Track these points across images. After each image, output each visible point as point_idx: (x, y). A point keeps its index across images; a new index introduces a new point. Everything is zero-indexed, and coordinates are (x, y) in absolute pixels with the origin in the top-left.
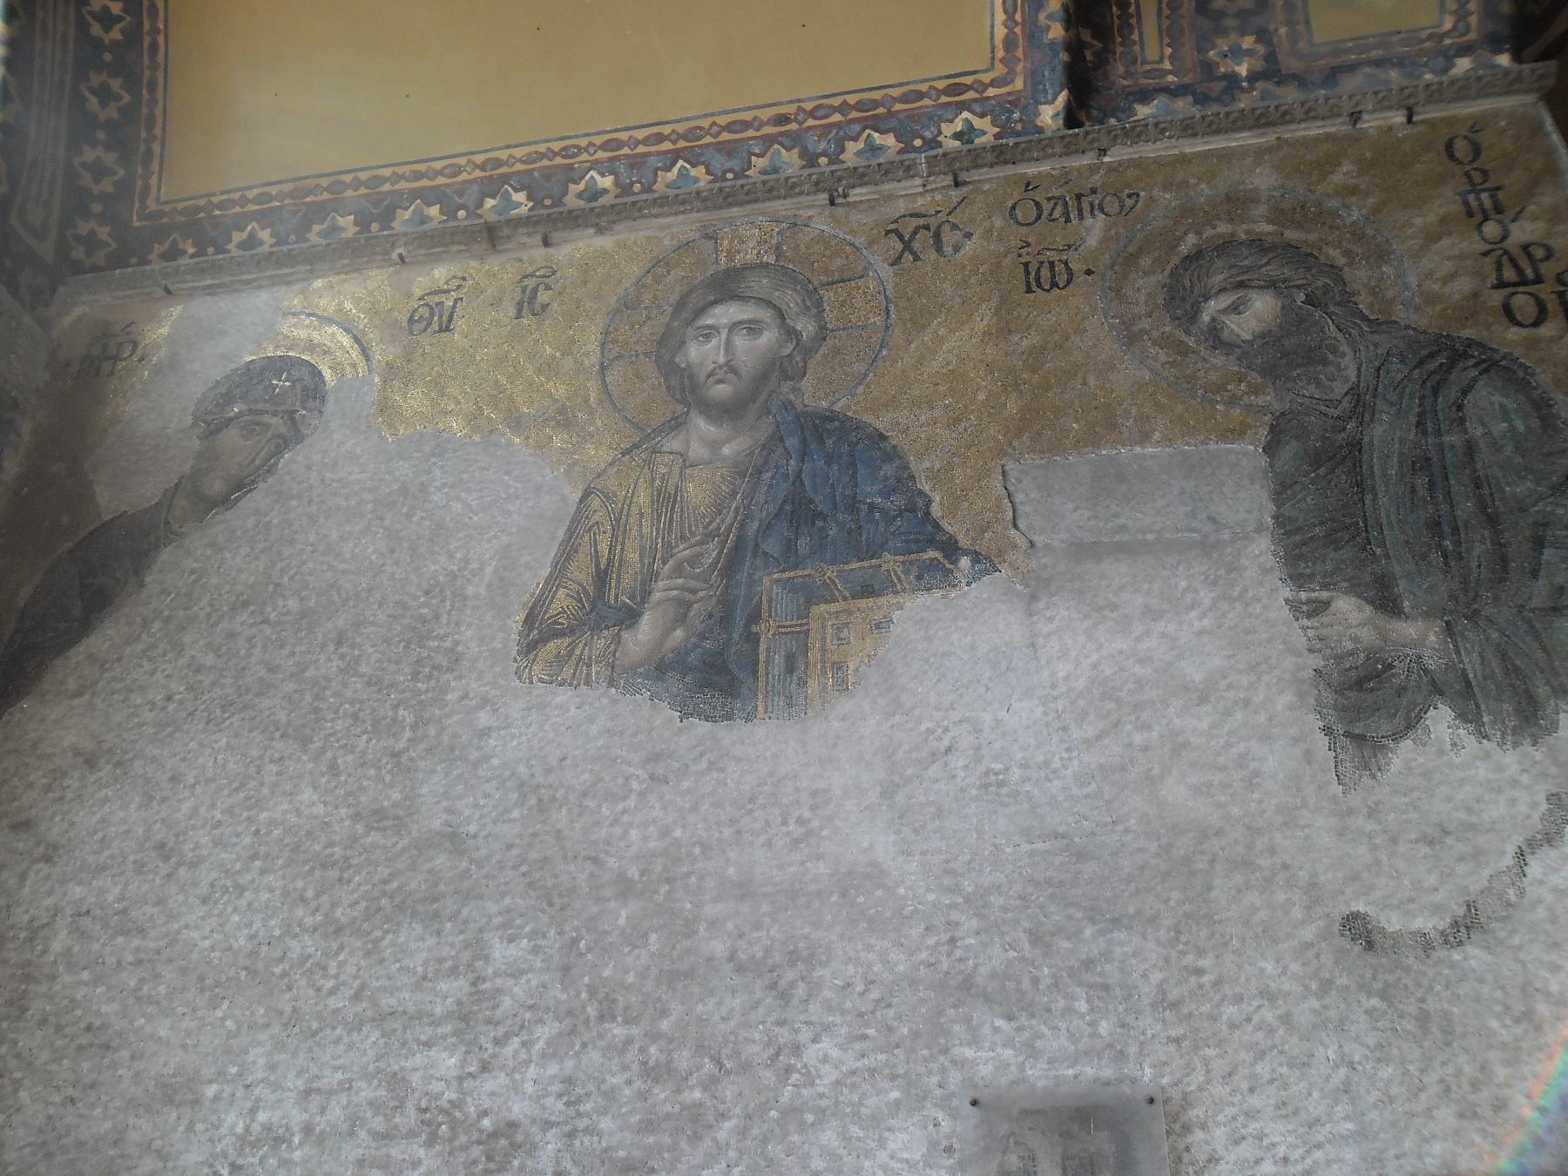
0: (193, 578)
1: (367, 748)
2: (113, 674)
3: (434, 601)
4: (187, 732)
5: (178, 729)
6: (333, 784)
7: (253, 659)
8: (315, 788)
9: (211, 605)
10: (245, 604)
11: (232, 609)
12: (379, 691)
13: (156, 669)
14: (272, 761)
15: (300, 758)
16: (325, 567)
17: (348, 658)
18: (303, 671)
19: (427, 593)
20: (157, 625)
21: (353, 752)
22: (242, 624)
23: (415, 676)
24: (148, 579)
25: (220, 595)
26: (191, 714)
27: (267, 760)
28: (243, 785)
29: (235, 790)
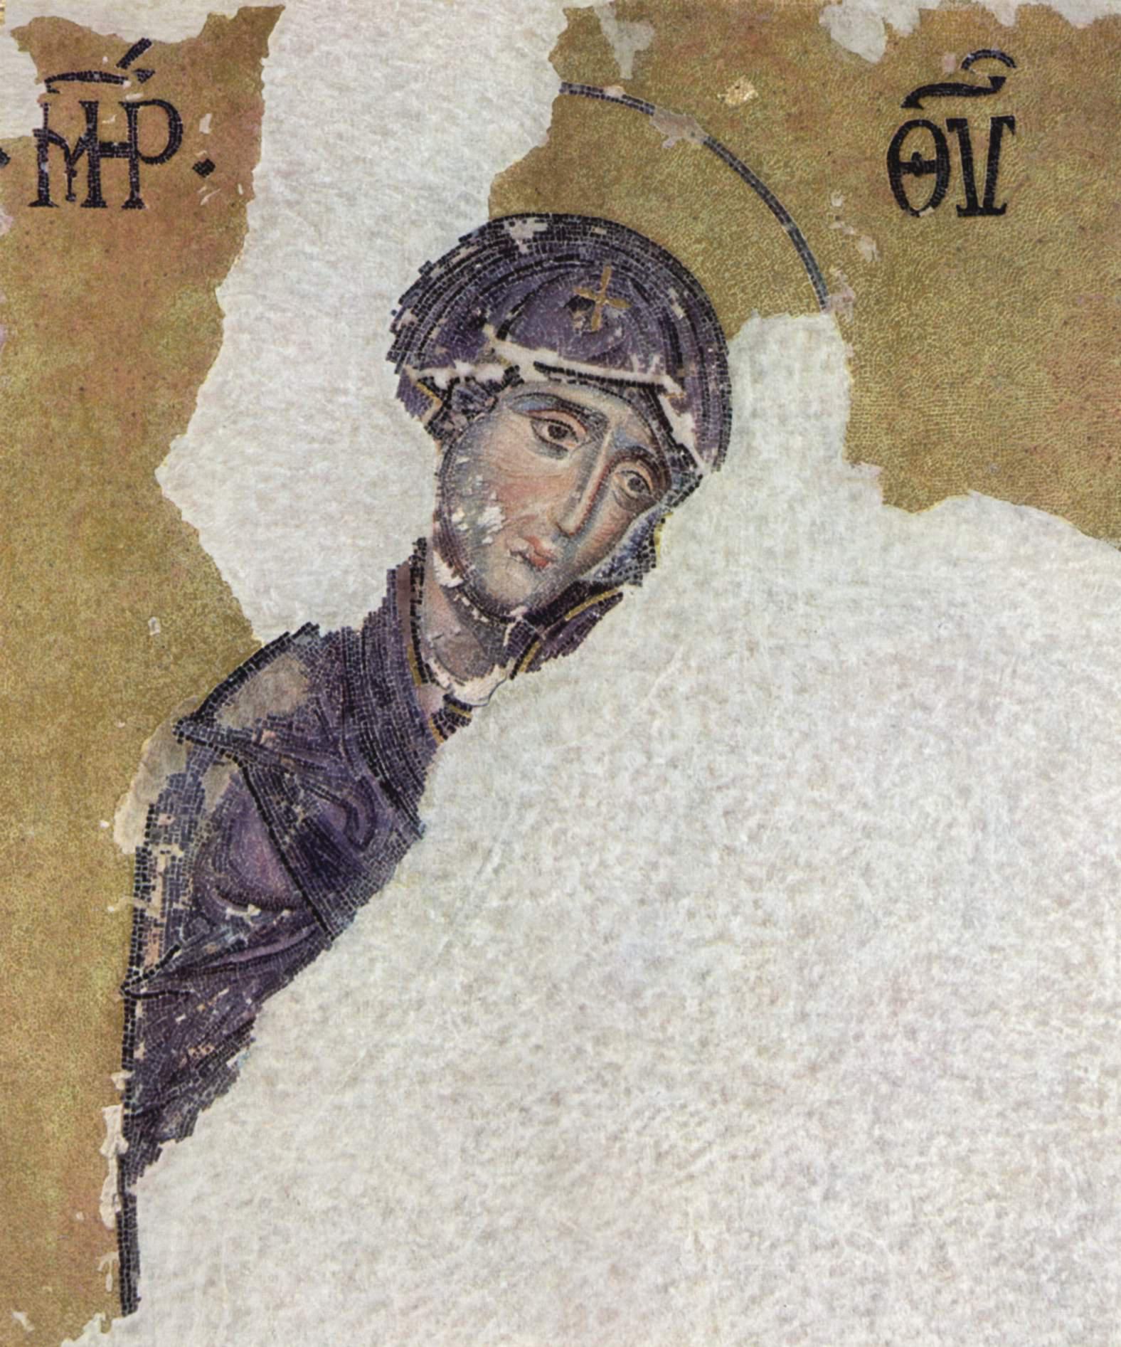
0: (531, 817)
1: (1000, 1228)
2: (411, 1036)
3: (1080, 924)
4: (619, 1175)
5: (595, 1170)
6: (946, 1298)
7: (719, 1023)
8: (915, 1306)
9: (589, 888)
10: (670, 892)
11: (642, 902)
12: (1001, 1115)
13: (506, 1028)
14: (816, 1248)
15: (871, 1244)
16: (824, 816)
17: (923, 1036)
18: (834, 1058)
19: (1062, 902)
20: (480, 930)
21: (974, 1235)
22: (676, 936)
23: (1072, 1085)
24: (426, 814)
25: (602, 864)
26: (615, 1138)
27: (805, 1244)
28: (766, 1291)
29: (753, 1300)
